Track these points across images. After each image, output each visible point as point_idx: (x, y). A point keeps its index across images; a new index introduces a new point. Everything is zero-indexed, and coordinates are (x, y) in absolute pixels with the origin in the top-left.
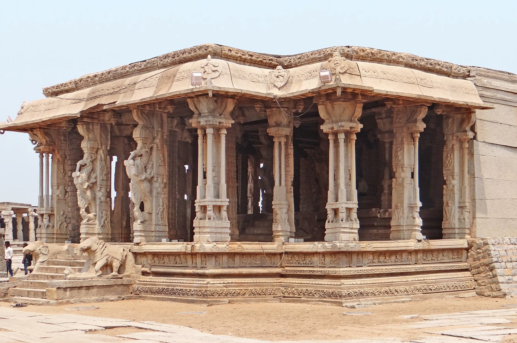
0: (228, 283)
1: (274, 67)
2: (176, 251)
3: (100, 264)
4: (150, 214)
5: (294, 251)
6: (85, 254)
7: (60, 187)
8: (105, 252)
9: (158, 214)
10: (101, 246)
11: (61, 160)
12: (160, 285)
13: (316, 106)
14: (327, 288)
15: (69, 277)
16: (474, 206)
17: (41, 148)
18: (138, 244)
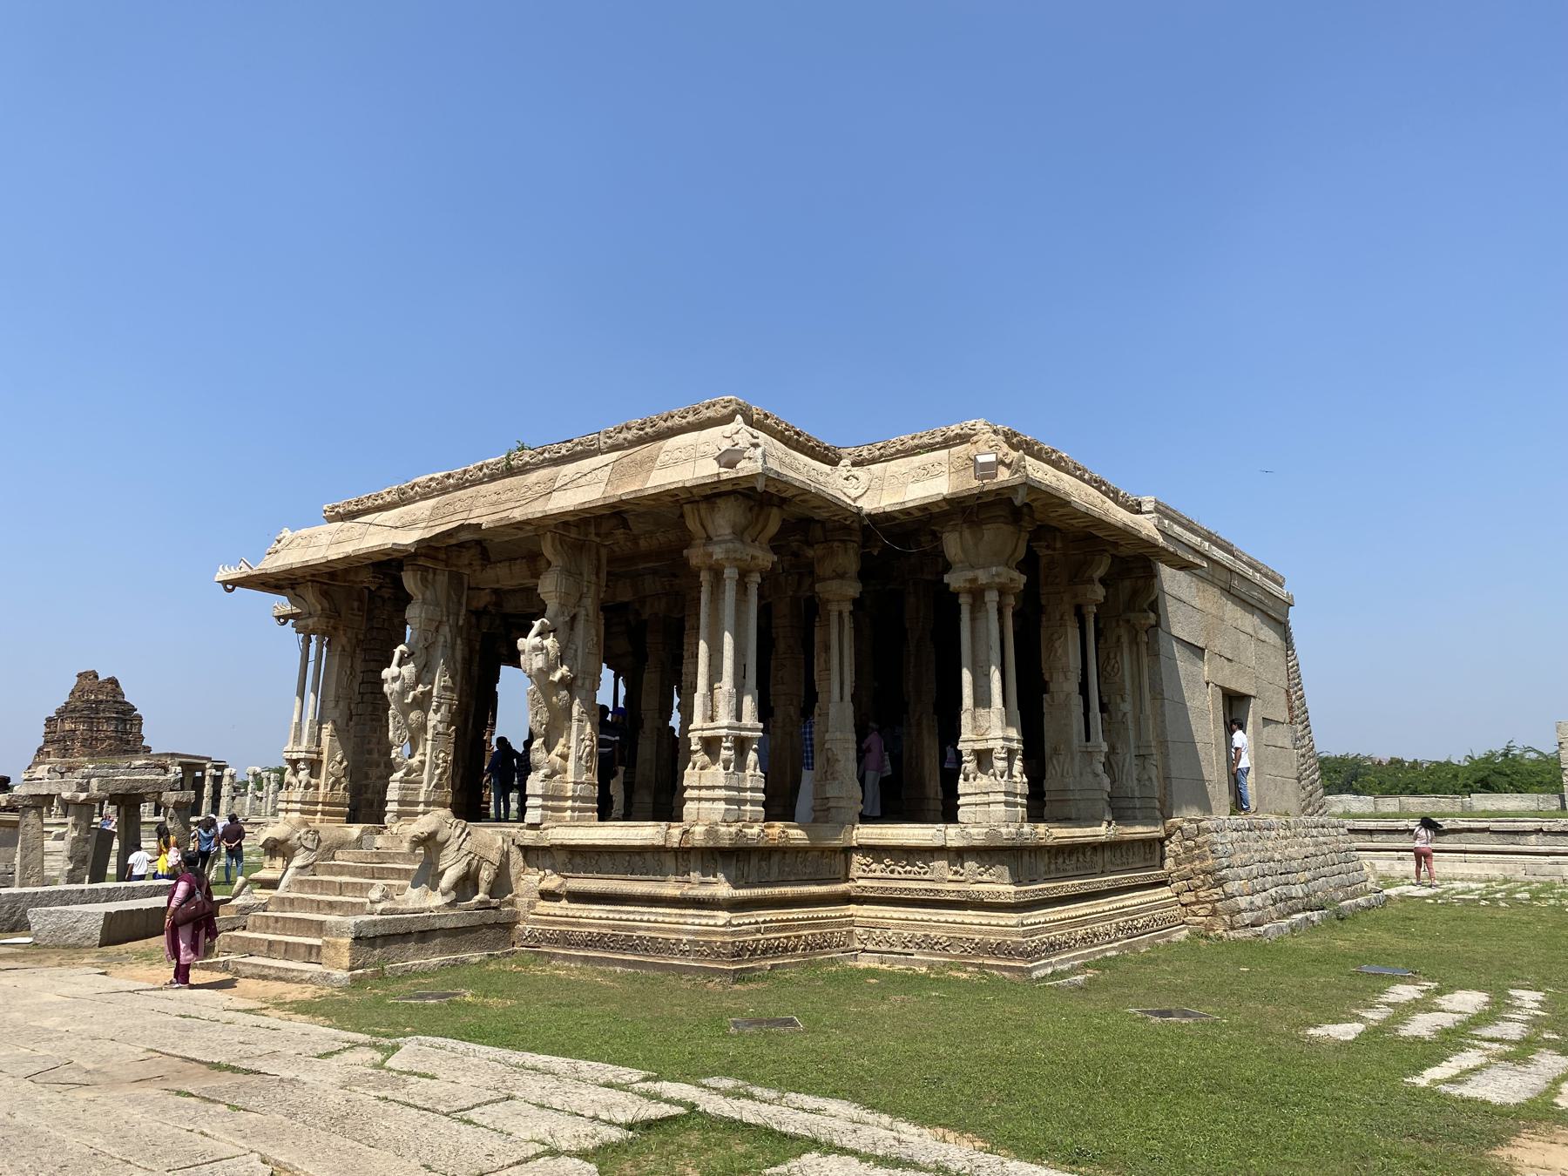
0: (764, 922)
1: (834, 462)
2: (638, 843)
4: (565, 757)
5: (882, 842)
7: (341, 704)
8: (467, 846)
10: (459, 831)
13: (936, 537)
14: (980, 932)
15: (379, 907)
17: (310, 622)
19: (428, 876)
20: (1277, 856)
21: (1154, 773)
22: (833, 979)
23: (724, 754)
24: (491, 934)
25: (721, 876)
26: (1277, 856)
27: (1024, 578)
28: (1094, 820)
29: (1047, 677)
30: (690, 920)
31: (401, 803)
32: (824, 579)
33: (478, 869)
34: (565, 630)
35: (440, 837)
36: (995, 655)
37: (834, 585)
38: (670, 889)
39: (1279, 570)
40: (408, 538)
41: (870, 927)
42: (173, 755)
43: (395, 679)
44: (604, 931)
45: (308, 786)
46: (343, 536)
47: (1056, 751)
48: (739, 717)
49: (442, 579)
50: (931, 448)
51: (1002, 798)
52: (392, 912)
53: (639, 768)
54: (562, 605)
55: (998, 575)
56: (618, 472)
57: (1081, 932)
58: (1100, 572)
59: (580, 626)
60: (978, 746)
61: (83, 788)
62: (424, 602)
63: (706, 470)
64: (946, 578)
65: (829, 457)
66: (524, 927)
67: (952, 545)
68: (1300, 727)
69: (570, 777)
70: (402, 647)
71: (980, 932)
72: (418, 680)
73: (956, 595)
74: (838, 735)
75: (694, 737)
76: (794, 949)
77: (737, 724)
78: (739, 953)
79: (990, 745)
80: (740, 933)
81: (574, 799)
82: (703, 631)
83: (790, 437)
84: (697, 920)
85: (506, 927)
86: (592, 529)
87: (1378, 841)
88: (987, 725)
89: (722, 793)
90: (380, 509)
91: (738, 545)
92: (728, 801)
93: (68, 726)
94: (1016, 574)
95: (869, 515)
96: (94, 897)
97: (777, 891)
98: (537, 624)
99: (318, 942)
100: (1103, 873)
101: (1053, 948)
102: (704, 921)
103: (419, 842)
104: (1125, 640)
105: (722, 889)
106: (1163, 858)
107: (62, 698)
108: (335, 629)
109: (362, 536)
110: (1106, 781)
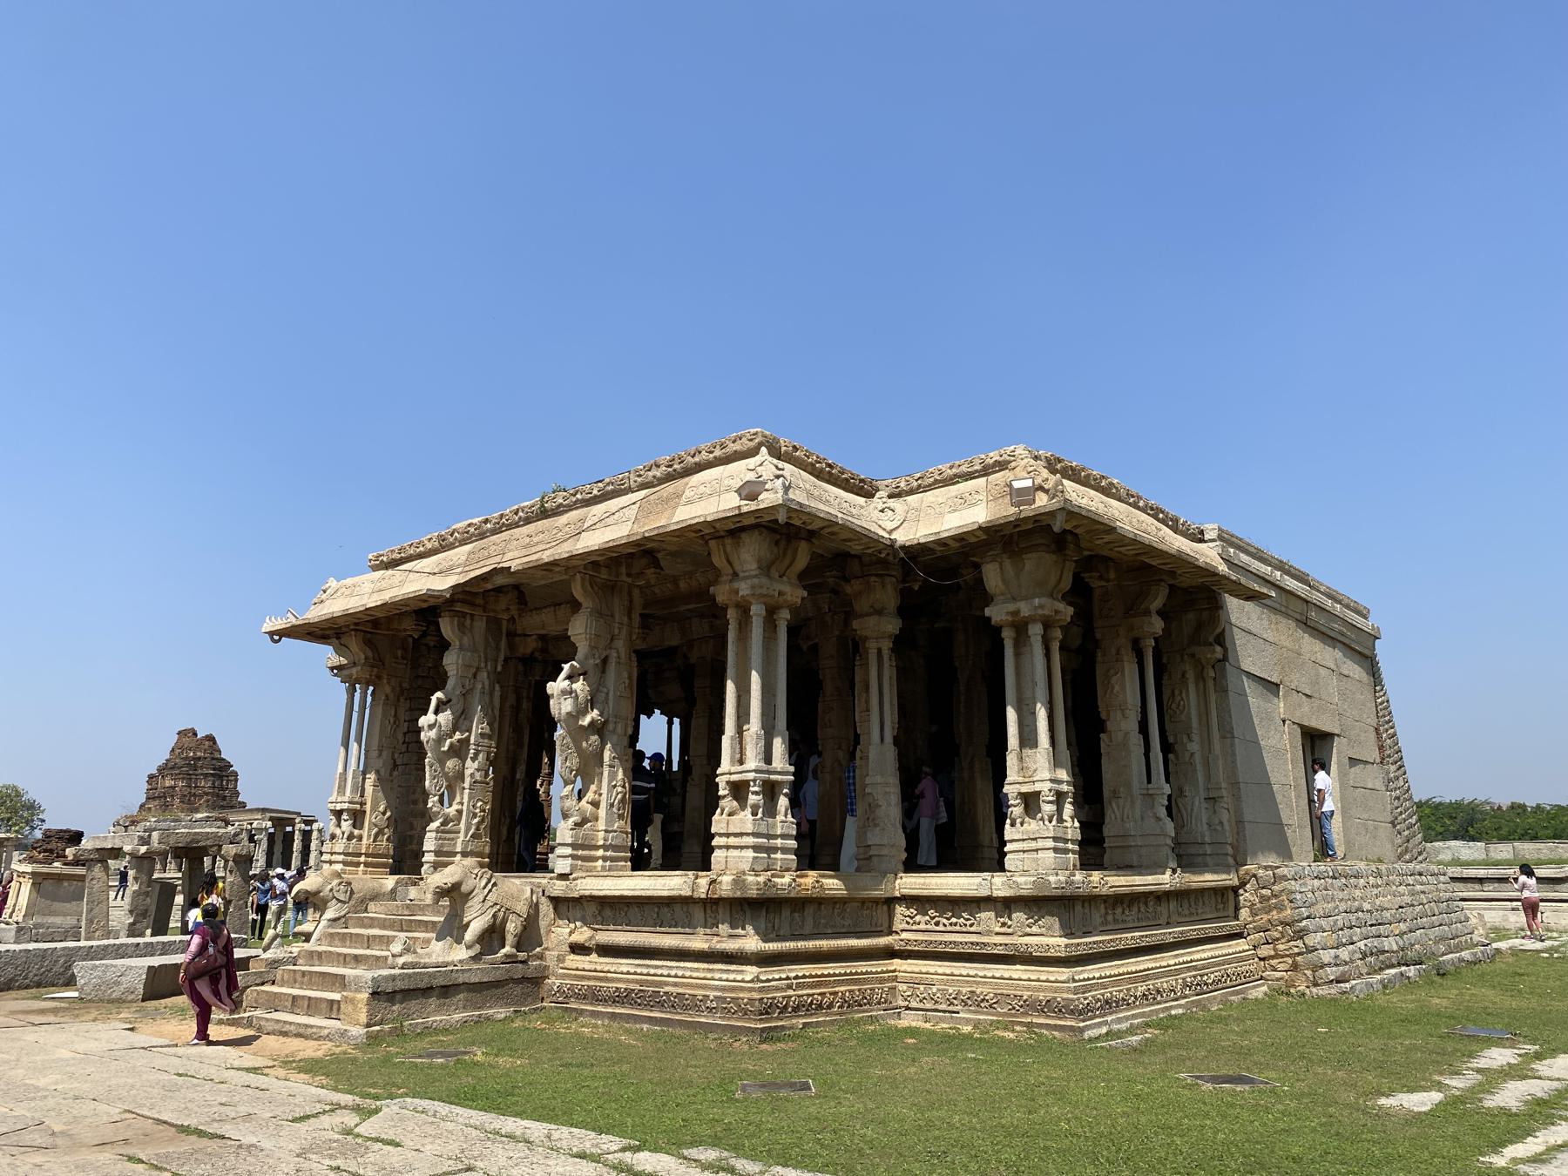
0: (797, 977)
1: (869, 495)
2: (665, 893)
3: (476, 927)
4: (596, 804)
5: (925, 893)
6: (445, 902)
7: (385, 753)
8: (492, 898)
9: (612, 805)
10: (484, 882)
11: (392, 697)
12: (619, 980)
13: (977, 566)
14: (1028, 989)
15: (401, 961)
16: (1237, 797)
17: (354, 671)
18: (563, 877)
19: (453, 928)
20: (1366, 906)
21: (1225, 817)
22: (870, 1039)
23: (752, 799)
24: (518, 989)
25: (749, 928)
26: (1366, 906)
27: (1070, 610)
28: (1158, 868)
29: (1103, 716)
30: (717, 976)
31: (438, 853)
32: (861, 616)
33: (505, 921)
34: (596, 673)
35: (464, 888)
36: (1041, 690)
37: (871, 621)
38: (698, 943)
39: (1363, 601)
40: (443, 584)
41: (913, 983)
42: (264, 810)
43: (431, 727)
44: (631, 986)
45: (350, 837)
46: (384, 584)
47: (1115, 794)
48: (768, 759)
49: (480, 625)
50: (969, 476)
51: (1050, 844)
52: (414, 966)
53: (669, 816)
54: (592, 648)
55: (1041, 606)
56: (644, 510)
57: (1142, 988)
58: (1157, 603)
59: (612, 667)
60: (1025, 789)
61: (144, 841)
62: (461, 648)
63: (729, 503)
64: (987, 612)
65: (864, 489)
66: (553, 982)
67: (993, 576)
68: (1393, 768)
69: (601, 825)
70: (439, 694)
71: (1028, 989)
72: (455, 727)
73: (998, 629)
74: (879, 779)
75: (721, 781)
76: (830, 1006)
77: (765, 767)
78: (767, 1010)
79: (1037, 787)
80: (769, 990)
81: (605, 847)
82: (730, 670)
83: (822, 470)
84: (724, 975)
85: (535, 982)
86: (623, 570)
87: (1490, 891)
88: (1035, 767)
89: (750, 840)
90: (421, 556)
91: (764, 580)
92: (756, 848)
93: (168, 783)
94: (1061, 606)
95: (903, 547)
96: (139, 951)
97: (811, 944)
98: (566, 667)
99: (336, 996)
100: (1168, 925)
101: (1109, 1005)
102: (731, 977)
103: (442, 893)
104: (1191, 676)
105: (751, 942)
106: (1237, 909)
107: (162, 756)
108: (379, 677)
109: (402, 583)
110: (1170, 826)
